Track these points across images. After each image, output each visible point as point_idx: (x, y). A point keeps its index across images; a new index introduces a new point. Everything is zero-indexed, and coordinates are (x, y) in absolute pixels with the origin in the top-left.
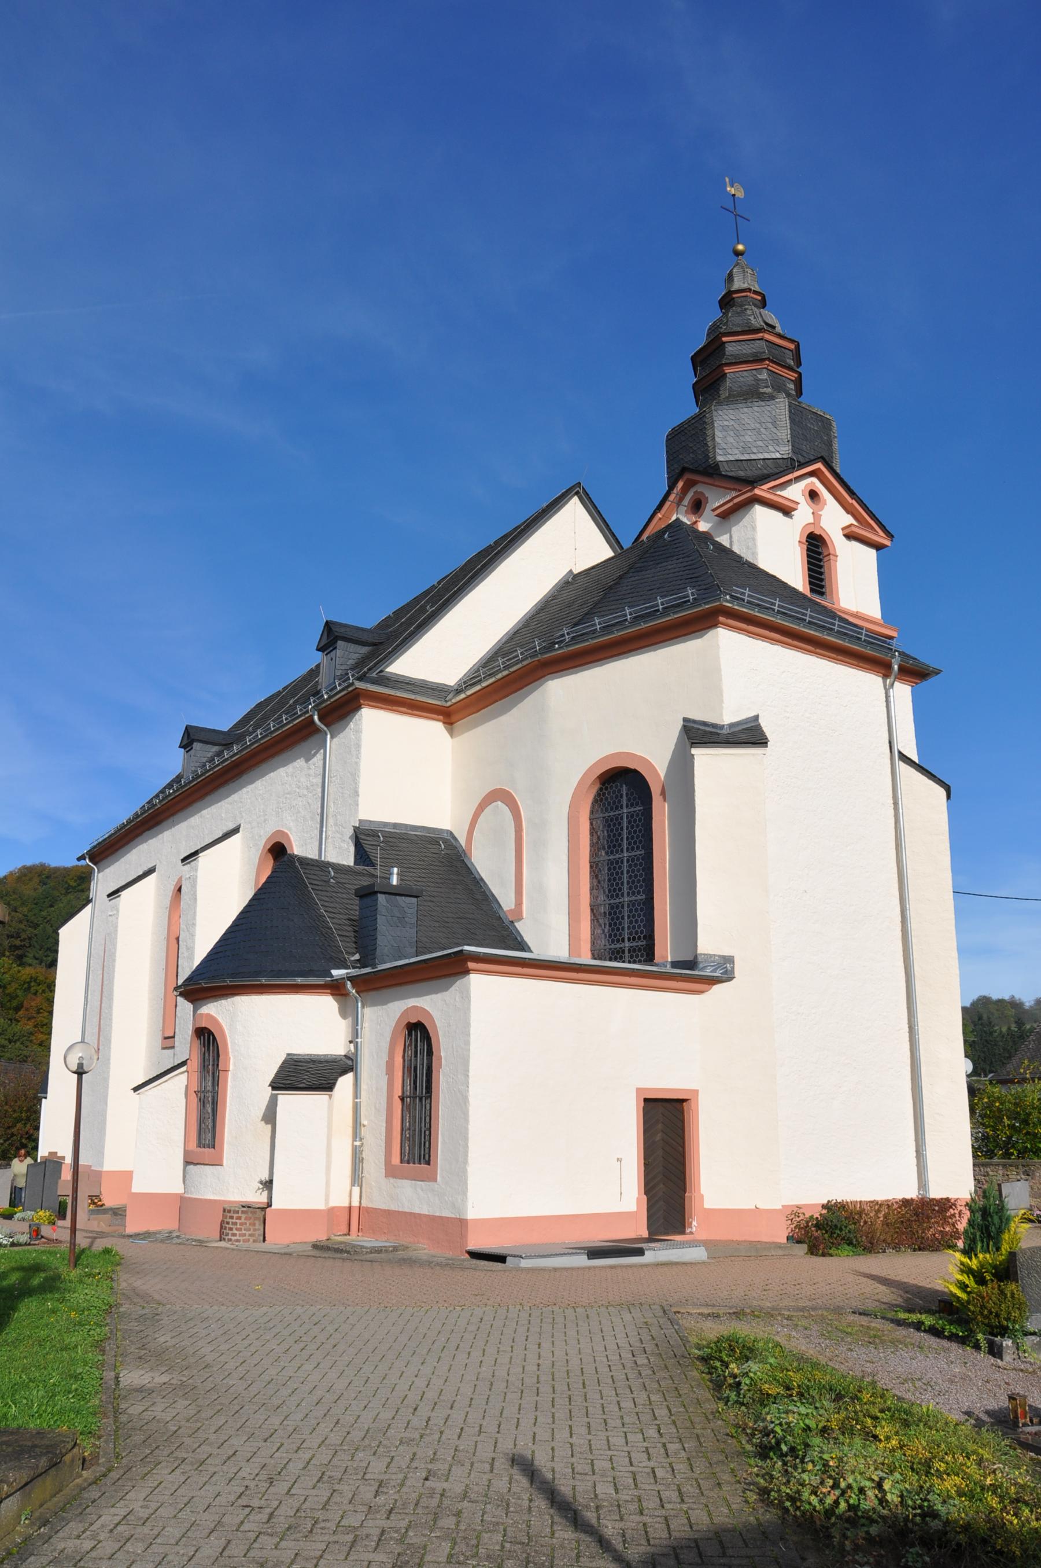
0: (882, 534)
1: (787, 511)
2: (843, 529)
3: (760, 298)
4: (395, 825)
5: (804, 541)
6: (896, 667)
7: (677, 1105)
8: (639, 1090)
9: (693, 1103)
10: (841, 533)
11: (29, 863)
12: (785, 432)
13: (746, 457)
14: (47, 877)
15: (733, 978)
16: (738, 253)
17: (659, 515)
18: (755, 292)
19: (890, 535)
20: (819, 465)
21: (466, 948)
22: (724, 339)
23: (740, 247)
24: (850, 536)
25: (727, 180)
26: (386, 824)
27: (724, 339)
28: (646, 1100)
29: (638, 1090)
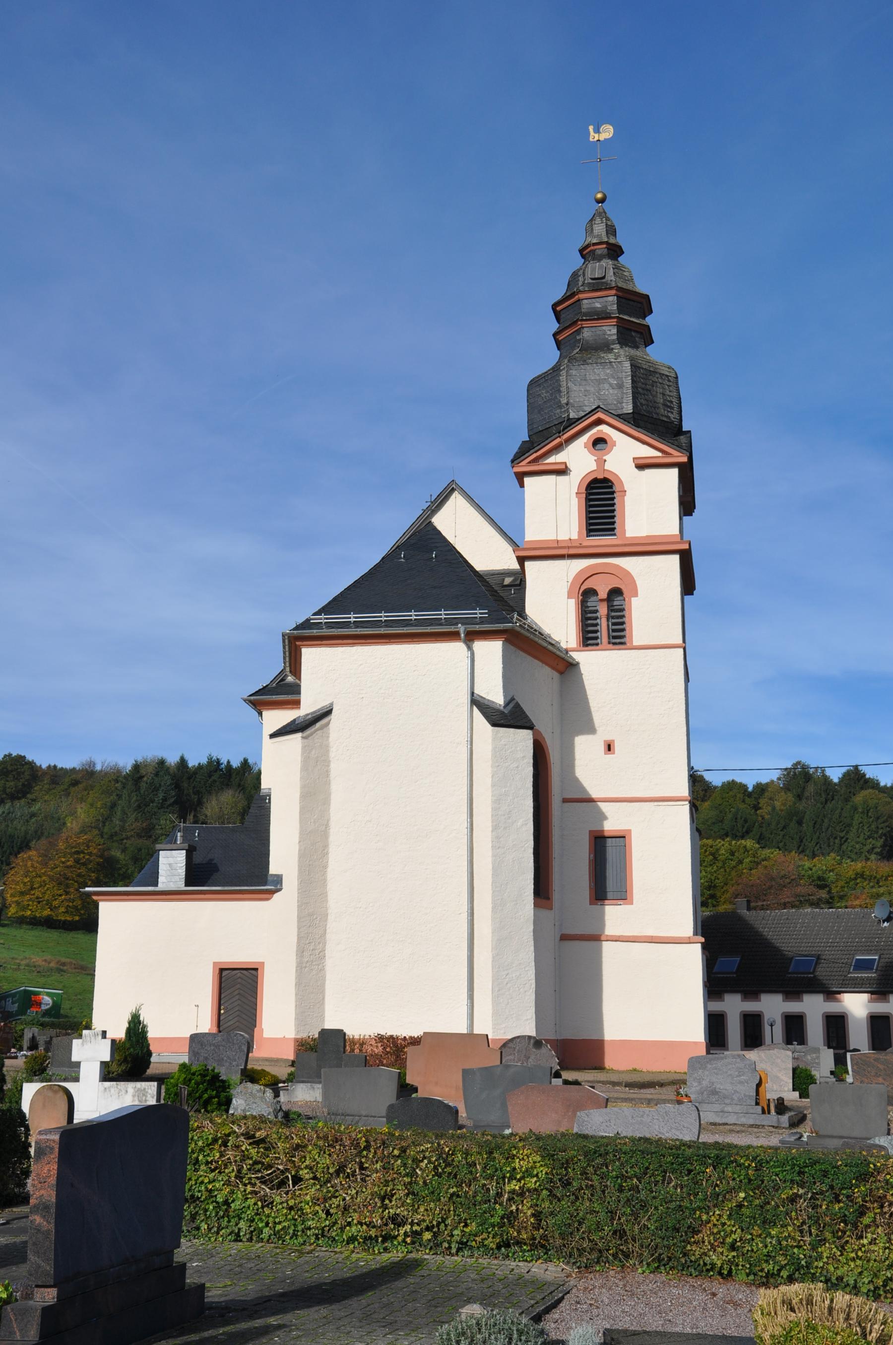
1: (562, 471)
3: (605, 246)
5: (584, 490)
7: (253, 972)
9: (259, 971)
15: (280, 890)
16: (602, 201)
18: (594, 244)
21: (87, 889)
22: (558, 309)
23: (599, 196)
25: (591, 128)
27: (558, 309)
28: (222, 970)
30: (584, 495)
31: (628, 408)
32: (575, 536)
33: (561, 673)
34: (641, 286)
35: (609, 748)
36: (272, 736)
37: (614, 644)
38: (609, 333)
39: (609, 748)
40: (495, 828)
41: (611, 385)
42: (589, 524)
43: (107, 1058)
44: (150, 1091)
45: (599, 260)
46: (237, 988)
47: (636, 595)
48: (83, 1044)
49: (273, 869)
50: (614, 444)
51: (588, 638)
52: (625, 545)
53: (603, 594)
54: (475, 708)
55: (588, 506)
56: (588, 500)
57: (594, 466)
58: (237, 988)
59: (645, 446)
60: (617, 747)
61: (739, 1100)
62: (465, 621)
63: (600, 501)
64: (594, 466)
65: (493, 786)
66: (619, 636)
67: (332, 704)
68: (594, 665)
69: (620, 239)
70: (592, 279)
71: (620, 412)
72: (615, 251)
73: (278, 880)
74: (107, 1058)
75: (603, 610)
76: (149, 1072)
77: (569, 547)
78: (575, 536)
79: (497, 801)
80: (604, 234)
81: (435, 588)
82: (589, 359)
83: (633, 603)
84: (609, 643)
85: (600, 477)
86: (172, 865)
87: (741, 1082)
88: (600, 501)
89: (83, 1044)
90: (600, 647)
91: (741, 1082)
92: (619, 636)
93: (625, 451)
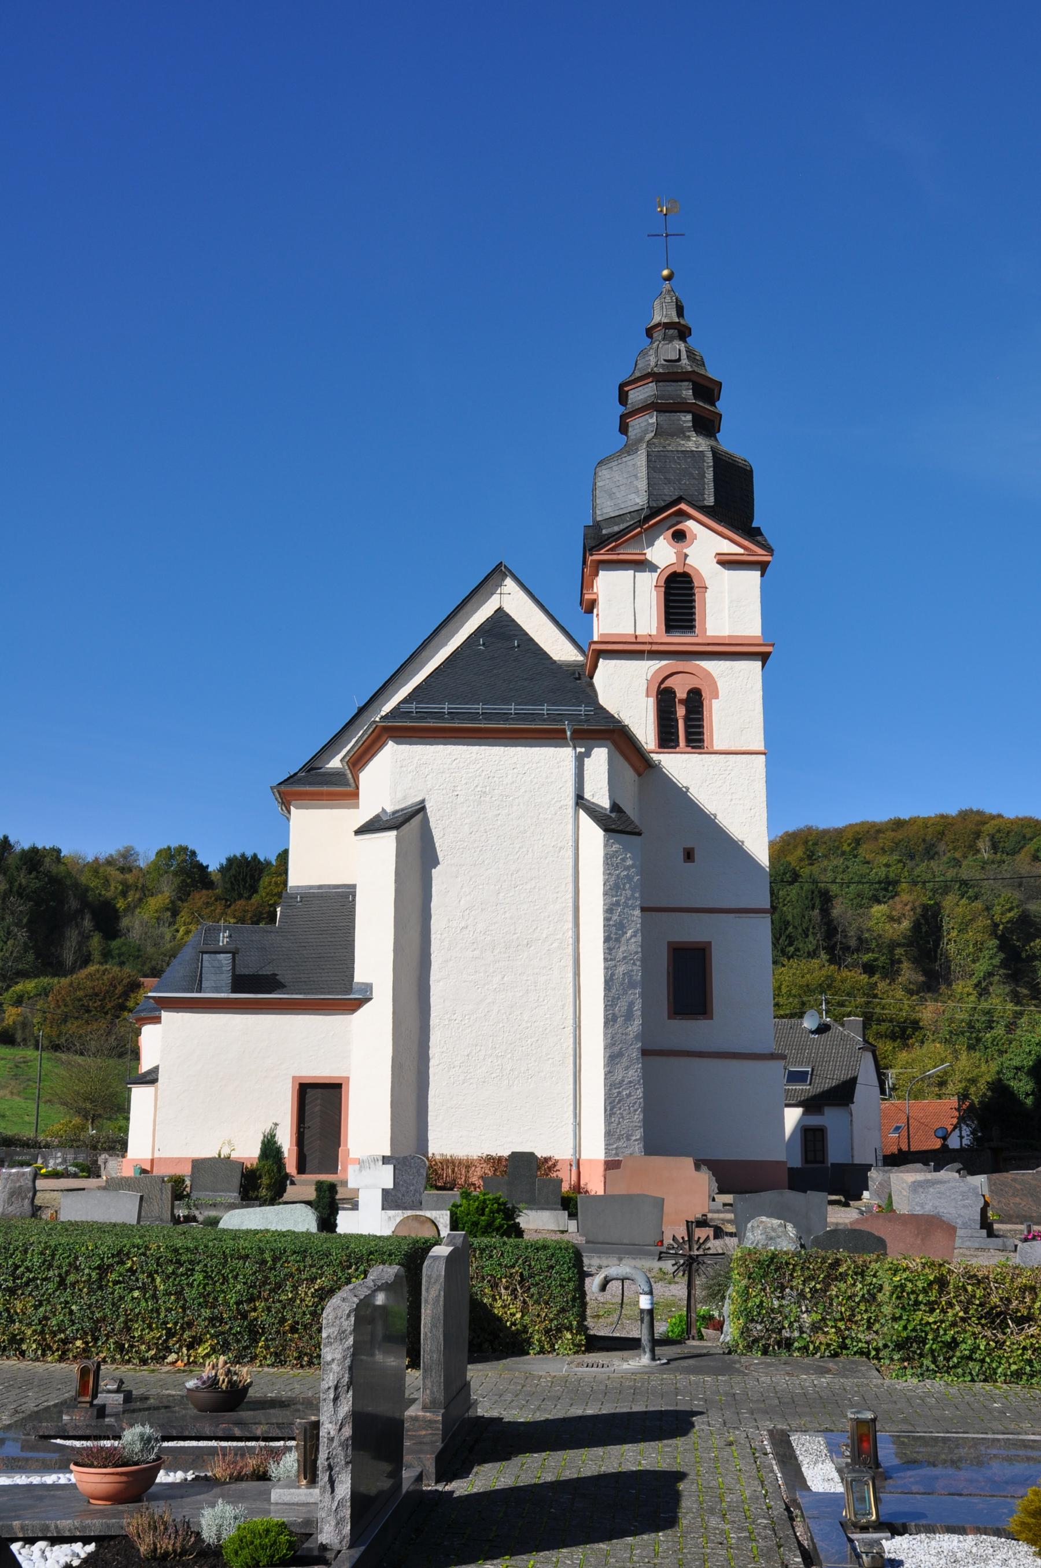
4: (320, 887)
5: (662, 583)
6: (569, 733)
8: (294, 1077)
10: (715, 561)
11: (791, 829)
12: (642, 485)
14: (815, 844)
15: (371, 999)
16: (668, 278)
19: (770, 550)
20: (683, 506)
22: (626, 389)
23: (665, 272)
24: (728, 563)
26: (311, 887)
27: (626, 389)
29: (294, 1077)
30: (663, 589)
31: (710, 501)
32: (654, 632)
33: (640, 775)
34: (712, 372)
35: (689, 855)
36: (358, 832)
37: (693, 747)
38: (683, 418)
39: (689, 855)
40: (607, 939)
41: (691, 474)
43: (390, 1185)
44: (441, 1220)
45: (671, 341)
46: (320, 1104)
47: (717, 697)
48: (360, 1170)
49: (359, 977)
50: (695, 537)
51: (667, 739)
52: (709, 644)
53: (681, 694)
54: (581, 811)
56: (667, 594)
58: (320, 1104)
59: (726, 541)
60: (697, 855)
61: (964, 1224)
62: (573, 718)
63: (680, 597)
65: (605, 894)
66: (696, 740)
67: (423, 801)
68: (678, 765)
69: (688, 320)
71: (701, 504)
72: (683, 333)
73: (368, 987)
74: (390, 1185)
75: (681, 711)
76: (286, 1197)
78: (654, 632)
79: (609, 911)
80: (674, 313)
81: (526, 679)
82: (669, 445)
85: (680, 570)
86: (218, 970)
87: (964, 1206)
88: (680, 597)
89: (360, 1170)
90: (678, 750)
91: (964, 1206)
92: (696, 740)
93: (706, 546)
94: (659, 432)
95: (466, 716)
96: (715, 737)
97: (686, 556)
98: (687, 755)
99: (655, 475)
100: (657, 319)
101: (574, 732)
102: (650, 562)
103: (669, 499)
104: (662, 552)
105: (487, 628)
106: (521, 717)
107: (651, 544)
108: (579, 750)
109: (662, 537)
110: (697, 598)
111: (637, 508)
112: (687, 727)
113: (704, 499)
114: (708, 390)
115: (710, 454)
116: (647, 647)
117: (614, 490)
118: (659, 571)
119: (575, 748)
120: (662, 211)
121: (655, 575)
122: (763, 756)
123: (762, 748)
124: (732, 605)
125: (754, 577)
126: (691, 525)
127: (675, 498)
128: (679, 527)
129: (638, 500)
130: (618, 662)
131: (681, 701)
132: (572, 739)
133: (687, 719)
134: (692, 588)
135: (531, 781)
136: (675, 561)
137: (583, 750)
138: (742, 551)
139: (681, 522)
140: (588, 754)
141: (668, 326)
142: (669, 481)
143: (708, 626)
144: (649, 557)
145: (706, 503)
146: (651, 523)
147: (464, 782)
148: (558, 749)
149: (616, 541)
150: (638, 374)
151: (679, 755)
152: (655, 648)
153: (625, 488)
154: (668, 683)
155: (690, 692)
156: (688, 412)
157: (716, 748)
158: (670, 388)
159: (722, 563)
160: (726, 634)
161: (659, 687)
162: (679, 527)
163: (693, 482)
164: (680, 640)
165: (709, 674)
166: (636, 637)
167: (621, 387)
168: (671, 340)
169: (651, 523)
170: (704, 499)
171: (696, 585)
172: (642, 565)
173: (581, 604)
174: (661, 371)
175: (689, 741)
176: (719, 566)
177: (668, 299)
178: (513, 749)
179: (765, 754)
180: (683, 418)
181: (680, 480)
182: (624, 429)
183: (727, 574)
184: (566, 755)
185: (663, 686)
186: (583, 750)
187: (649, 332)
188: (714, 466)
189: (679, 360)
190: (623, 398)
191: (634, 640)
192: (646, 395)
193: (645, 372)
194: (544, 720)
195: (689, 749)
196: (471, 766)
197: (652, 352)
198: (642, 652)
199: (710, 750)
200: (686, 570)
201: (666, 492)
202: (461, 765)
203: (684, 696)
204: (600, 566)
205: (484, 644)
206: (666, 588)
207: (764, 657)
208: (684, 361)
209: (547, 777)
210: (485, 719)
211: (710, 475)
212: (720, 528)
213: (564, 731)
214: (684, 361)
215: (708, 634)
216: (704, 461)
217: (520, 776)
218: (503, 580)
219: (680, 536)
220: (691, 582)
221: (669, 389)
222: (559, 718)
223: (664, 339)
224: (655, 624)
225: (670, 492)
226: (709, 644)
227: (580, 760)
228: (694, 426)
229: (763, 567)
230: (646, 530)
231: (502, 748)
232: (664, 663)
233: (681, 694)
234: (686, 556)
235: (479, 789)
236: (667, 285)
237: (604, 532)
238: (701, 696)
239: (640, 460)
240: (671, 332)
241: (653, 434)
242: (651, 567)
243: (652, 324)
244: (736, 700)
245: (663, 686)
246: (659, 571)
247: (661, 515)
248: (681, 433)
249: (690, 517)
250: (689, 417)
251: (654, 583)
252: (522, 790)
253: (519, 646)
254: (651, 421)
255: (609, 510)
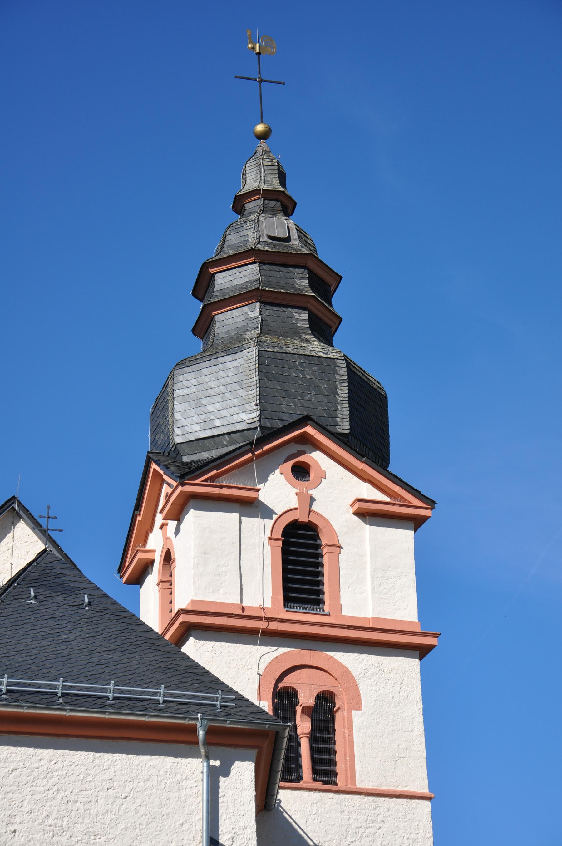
0: (416, 502)
2: (352, 505)
5: (278, 534)
6: (201, 733)
10: (351, 510)
13: (209, 433)
16: (264, 136)
17: (139, 518)
22: (212, 271)
23: (260, 128)
24: (368, 514)
27: (212, 271)
30: (280, 544)
31: (344, 427)
37: (325, 783)
38: (297, 316)
41: (319, 387)
42: (286, 590)
47: (359, 707)
50: (323, 475)
52: (349, 627)
53: (307, 699)
55: (285, 562)
56: (285, 552)
57: (294, 502)
64: (294, 502)
70: (270, 237)
75: (304, 726)
77: (268, 619)
78: (268, 604)
81: (115, 651)
82: (287, 345)
83: (354, 719)
84: (315, 780)
85: (303, 518)
94: (265, 328)
95: (38, 698)
96: (357, 768)
97: (312, 500)
98: (318, 795)
99: (270, 384)
100: (252, 182)
101: (209, 732)
102: (263, 504)
103: (289, 419)
104: (278, 491)
105: (34, 575)
106: (121, 703)
107: (264, 479)
108: (212, 762)
109: (278, 471)
110: (326, 560)
111: (240, 427)
112: (313, 751)
113: (336, 424)
114: (325, 283)
115: (343, 364)
116: (261, 625)
117: (204, 401)
118: (275, 517)
119: (207, 758)
120: (253, 48)
121: (269, 523)
122: (428, 804)
123: (423, 788)
124: (376, 573)
125: (404, 538)
126: (317, 458)
127: (295, 418)
128: (301, 458)
129: (244, 416)
130: (218, 643)
131: (305, 710)
132: (207, 743)
133: (313, 739)
134: (318, 546)
135: (136, 811)
136: (297, 506)
137: (217, 763)
138: (388, 499)
139: (303, 453)
140: (225, 771)
141: (268, 195)
142: (288, 394)
143: (344, 601)
144: (260, 496)
145: (339, 430)
146: (265, 448)
147: (26, 808)
148: (179, 760)
149: (217, 467)
150: (228, 252)
151: (306, 794)
152: (273, 626)
153: (217, 400)
154: (289, 681)
155: (319, 697)
156: (304, 309)
157: (360, 784)
158: (278, 273)
159: (362, 514)
160: (369, 614)
161: (276, 686)
162: (301, 458)
163: (321, 398)
164: (303, 619)
165: (346, 672)
166: (243, 609)
167: (206, 266)
168: (274, 213)
169: (265, 448)
170: (336, 424)
171: (324, 541)
172: (250, 506)
173: (121, 569)
174: (267, 248)
175: (317, 773)
176: (356, 518)
177: (267, 162)
178: (108, 756)
179: (429, 799)
180: (297, 316)
181: (302, 395)
182: (203, 327)
183: (369, 532)
184: (191, 770)
185: (281, 685)
186: (217, 763)
187: (239, 205)
188: (349, 381)
189: (288, 239)
190: (203, 284)
191: (240, 613)
192: (247, 279)
193: (247, 247)
194: (162, 710)
195: (319, 785)
196: (39, 782)
197: (249, 225)
198: (253, 632)
199: (350, 787)
200: (313, 518)
201: (284, 408)
202: (23, 779)
203: (311, 702)
204: (191, 502)
205: (35, 597)
206: (284, 543)
207: (422, 651)
208: (295, 242)
209: (161, 806)
210: (69, 704)
211: (343, 392)
212: (361, 466)
213: (193, 730)
214: (295, 242)
215: (345, 612)
216: (335, 372)
217: (119, 801)
218: (14, 524)
219: (301, 472)
220: (317, 537)
221: (277, 274)
222: (184, 708)
223: (263, 211)
224: (269, 593)
225: (290, 410)
226: (349, 627)
227: (214, 778)
228: (311, 328)
229: (416, 523)
230: (258, 456)
231: (91, 754)
232: (283, 650)
233: (307, 699)
234: (312, 500)
235: (50, 821)
236: (263, 145)
237: (185, 459)
238: (334, 703)
239: (246, 361)
240: (272, 203)
241: (258, 331)
242: (267, 513)
243: (245, 190)
244: (385, 712)
245: (281, 685)
246: (275, 517)
247: (276, 437)
248: (295, 333)
249: (317, 446)
250: (305, 315)
251: (268, 534)
252: (121, 826)
253: (90, 603)
254: (251, 315)
255: (197, 428)
